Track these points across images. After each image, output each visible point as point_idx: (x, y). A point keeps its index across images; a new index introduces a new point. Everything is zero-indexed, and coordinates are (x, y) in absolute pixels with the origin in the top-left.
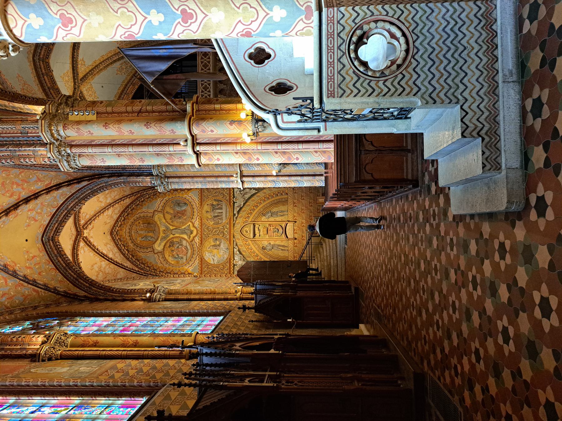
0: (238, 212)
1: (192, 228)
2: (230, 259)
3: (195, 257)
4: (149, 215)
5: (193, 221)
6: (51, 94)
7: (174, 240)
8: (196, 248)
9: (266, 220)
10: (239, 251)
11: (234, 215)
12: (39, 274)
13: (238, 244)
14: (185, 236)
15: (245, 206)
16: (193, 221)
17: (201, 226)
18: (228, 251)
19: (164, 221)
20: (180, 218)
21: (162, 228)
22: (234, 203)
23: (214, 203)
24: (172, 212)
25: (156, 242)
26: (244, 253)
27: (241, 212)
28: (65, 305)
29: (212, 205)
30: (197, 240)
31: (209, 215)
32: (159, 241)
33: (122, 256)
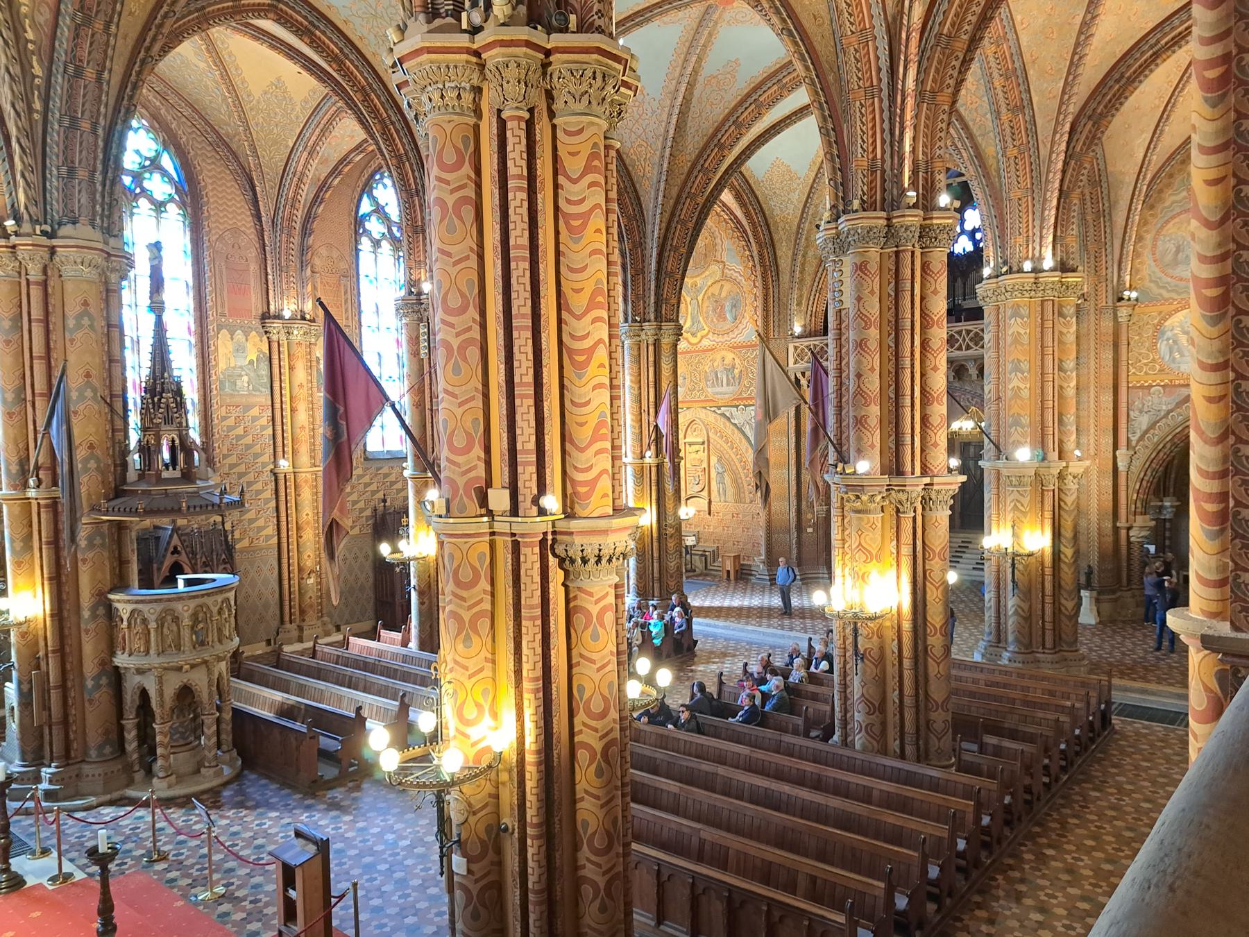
0: (723, 415)
1: (699, 335)
4: (718, 254)
5: (710, 336)
11: (719, 408)
16: (710, 336)
17: (704, 351)
20: (714, 310)
22: (737, 407)
23: (736, 371)
24: (723, 295)
27: (723, 420)
29: (733, 367)
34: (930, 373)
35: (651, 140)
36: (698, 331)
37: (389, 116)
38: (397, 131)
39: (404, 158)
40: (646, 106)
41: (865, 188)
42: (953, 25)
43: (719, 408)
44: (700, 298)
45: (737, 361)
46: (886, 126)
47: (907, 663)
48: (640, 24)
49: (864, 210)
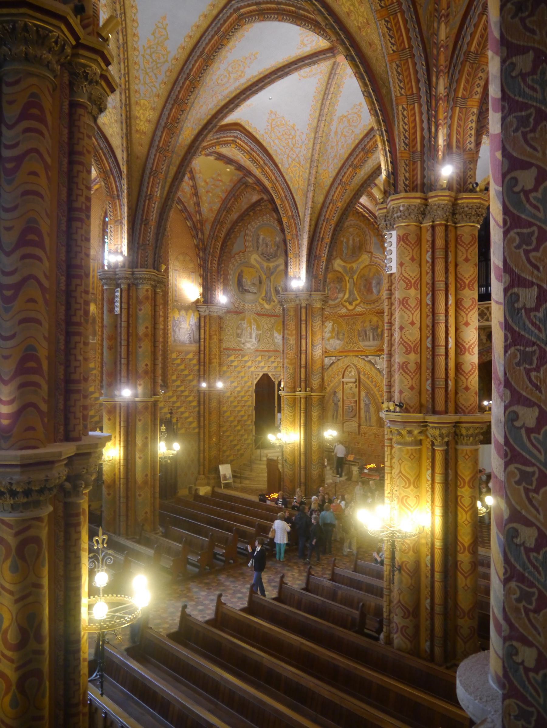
0: (370, 362)
1: (354, 303)
5: (361, 305)
7: (344, 283)
9: (362, 398)
10: (333, 363)
11: (367, 356)
12: (207, 192)
14: (347, 296)
15: (375, 370)
17: (357, 315)
19: (362, 267)
20: (365, 286)
21: (354, 265)
24: (371, 275)
25: (342, 259)
26: (330, 369)
28: (189, 224)
30: (344, 311)
31: (367, 324)
32: (342, 263)
34: (463, 327)
35: (303, 162)
36: (354, 300)
37: (99, 144)
38: (105, 154)
39: (110, 173)
40: (297, 138)
41: (407, 175)
42: (479, 44)
43: (367, 356)
44: (355, 277)
46: (425, 125)
47: (437, 576)
48: (281, 77)
49: (406, 191)
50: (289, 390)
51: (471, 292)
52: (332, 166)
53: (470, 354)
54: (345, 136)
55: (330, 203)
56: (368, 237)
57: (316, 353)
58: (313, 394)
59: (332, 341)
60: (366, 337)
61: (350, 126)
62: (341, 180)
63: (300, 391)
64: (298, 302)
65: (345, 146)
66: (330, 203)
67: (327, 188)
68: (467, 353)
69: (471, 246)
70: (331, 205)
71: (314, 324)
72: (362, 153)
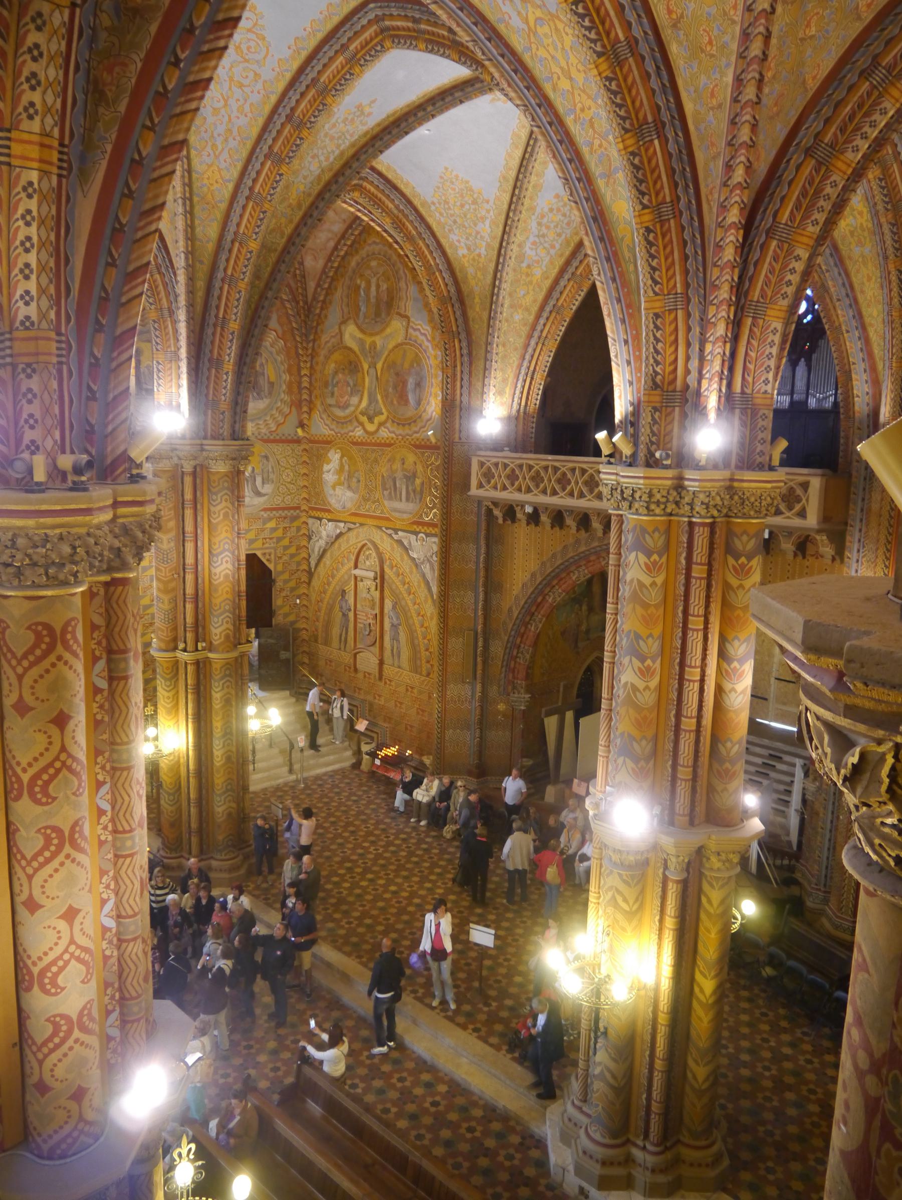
0: (400, 542)
2: (329, 511)
3: (333, 427)
5: (388, 425)
6: (303, 95)
7: (360, 375)
8: (346, 431)
9: (386, 611)
13: (351, 534)
14: (364, 404)
18: (340, 509)
19: (390, 346)
20: (395, 387)
21: (379, 340)
22: (416, 533)
23: (418, 482)
26: (336, 545)
29: (414, 475)
30: (359, 433)
31: (397, 465)
32: (359, 335)
33: (332, 244)
43: (396, 531)
44: (379, 366)
45: (420, 468)
50: (163, 646)
51: (39, 809)
52: (225, 155)
53: (47, 992)
54: (241, 86)
55: (233, 242)
56: (402, 284)
57: (218, 570)
58: (211, 655)
59: (339, 491)
60: (394, 494)
61: (246, 61)
62: (251, 189)
63: (185, 650)
64: (175, 460)
65: (247, 108)
66: (233, 242)
67: (223, 206)
68: (36, 988)
69: (32, 665)
70: (237, 245)
71: (212, 509)
72: (288, 128)
